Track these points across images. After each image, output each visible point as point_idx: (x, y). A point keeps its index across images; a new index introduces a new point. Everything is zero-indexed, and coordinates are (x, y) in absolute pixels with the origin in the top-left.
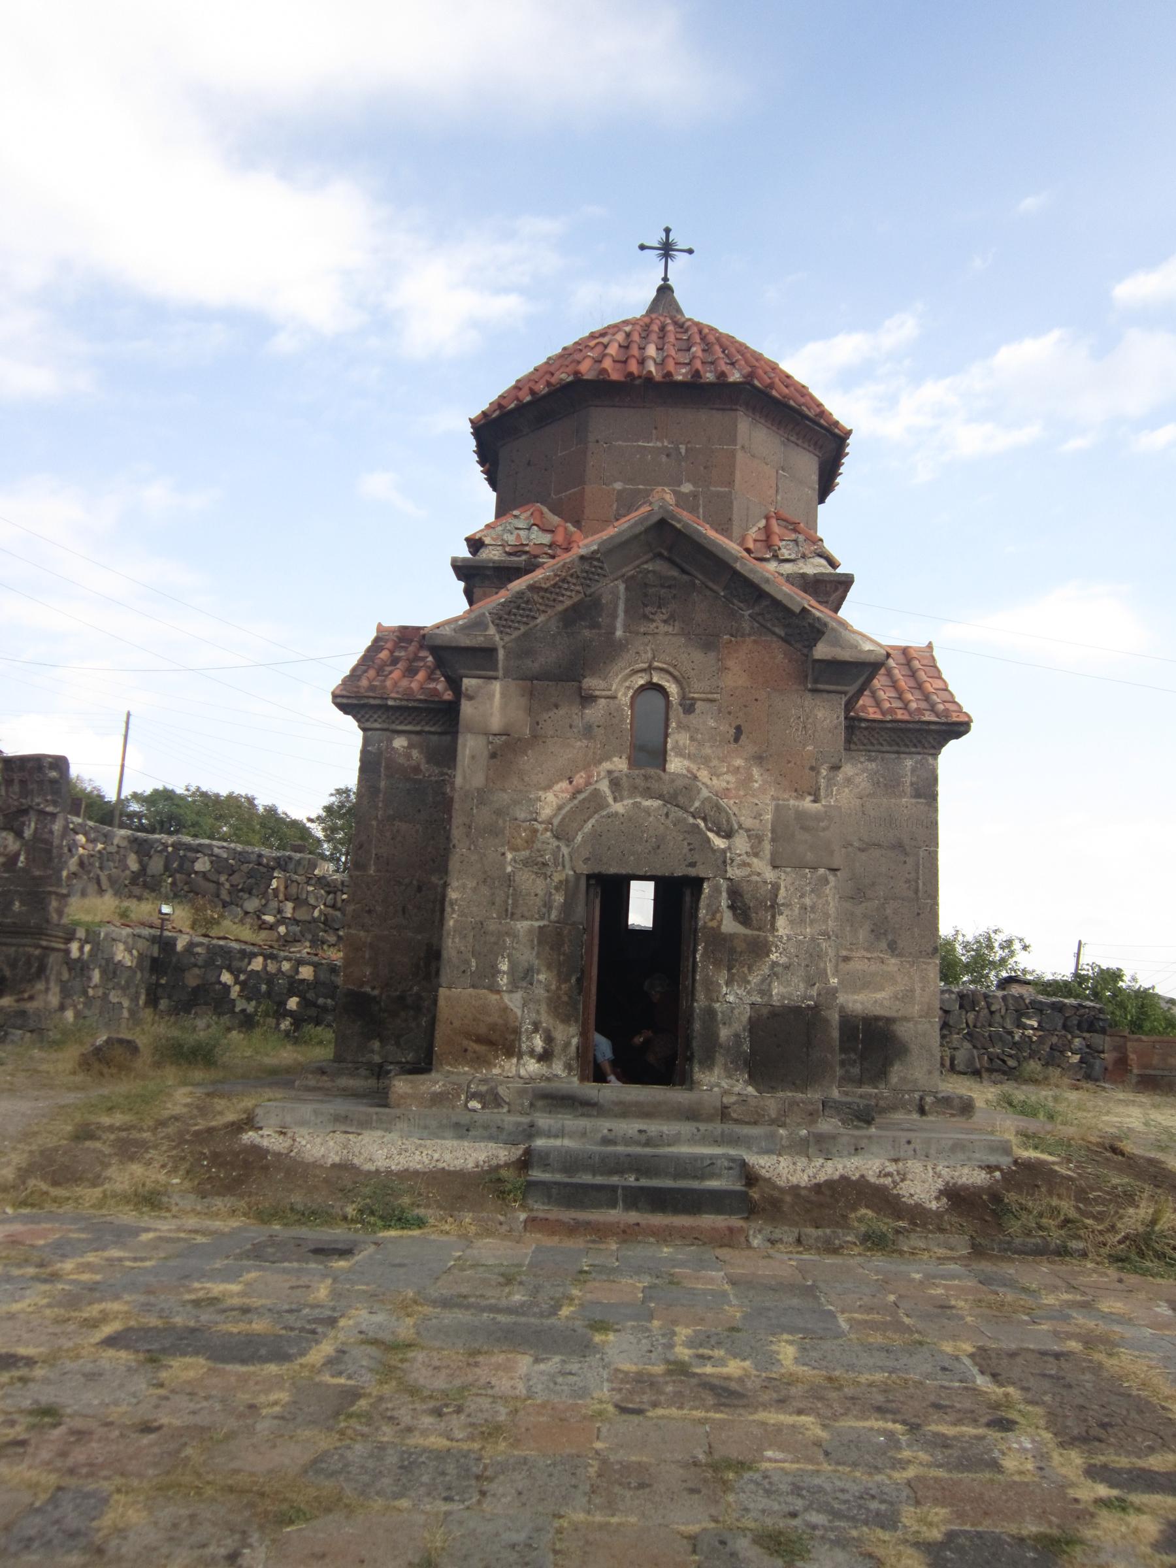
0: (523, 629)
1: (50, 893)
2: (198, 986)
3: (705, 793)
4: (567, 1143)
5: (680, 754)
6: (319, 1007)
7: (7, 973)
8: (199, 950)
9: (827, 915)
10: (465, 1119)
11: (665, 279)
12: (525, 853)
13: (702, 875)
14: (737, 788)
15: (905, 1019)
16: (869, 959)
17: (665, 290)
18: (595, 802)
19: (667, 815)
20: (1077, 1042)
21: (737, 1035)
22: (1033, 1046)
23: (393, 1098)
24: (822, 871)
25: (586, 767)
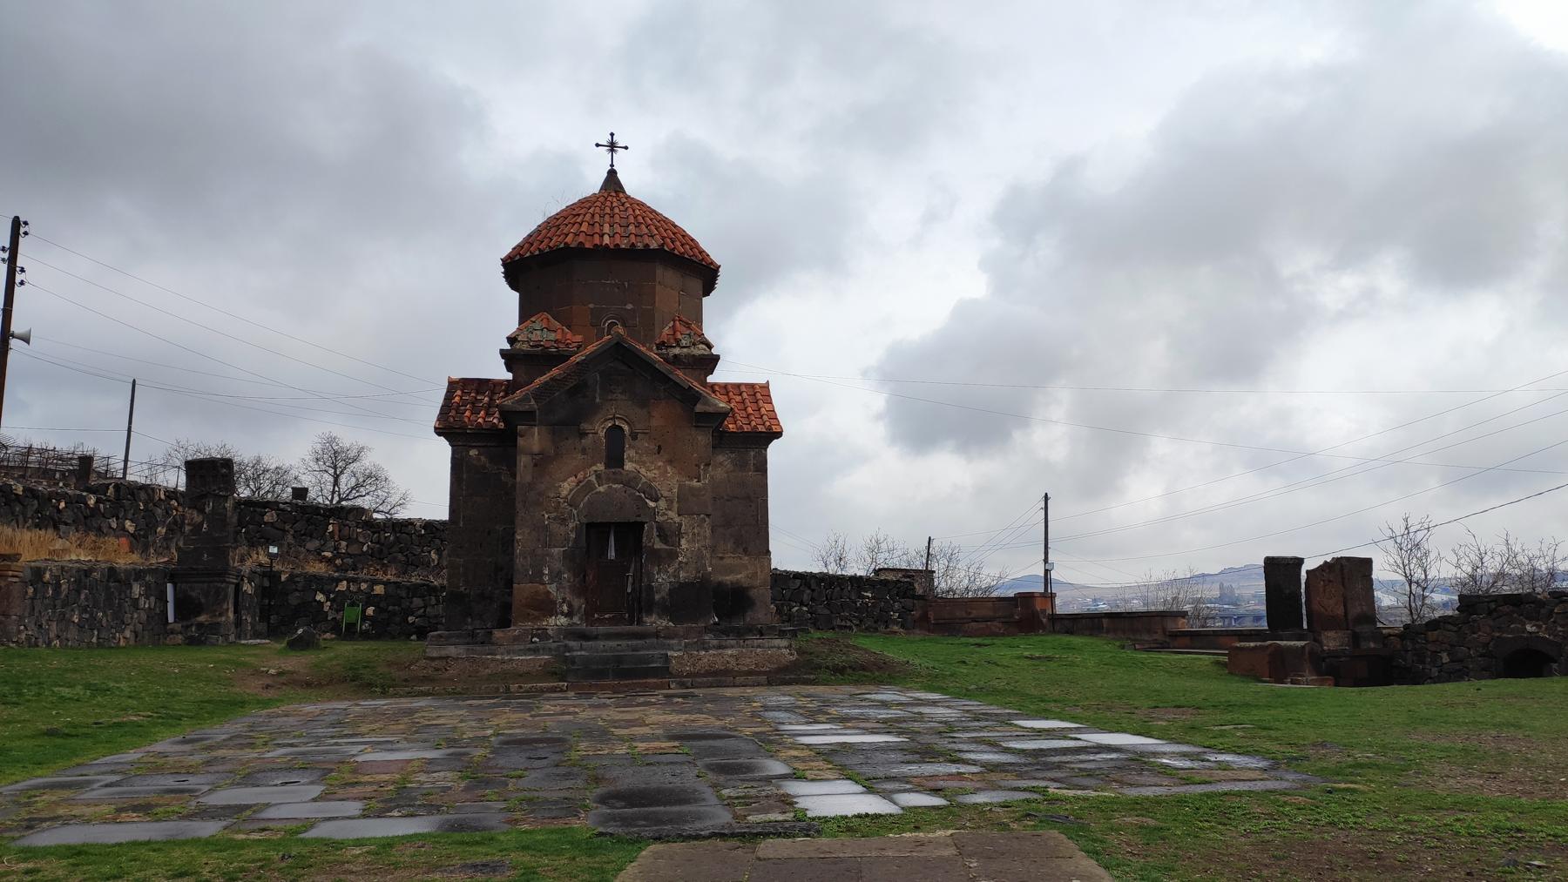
0: (548, 399)
2: (299, 604)
3: (644, 480)
4: (583, 653)
5: (631, 461)
7: (203, 601)
9: (705, 537)
10: (532, 646)
11: (612, 165)
13: (644, 521)
16: (734, 558)
17: (612, 173)
18: (589, 487)
20: (897, 605)
21: (663, 598)
23: (494, 640)
24: (702, 516)
25: (584, 469)
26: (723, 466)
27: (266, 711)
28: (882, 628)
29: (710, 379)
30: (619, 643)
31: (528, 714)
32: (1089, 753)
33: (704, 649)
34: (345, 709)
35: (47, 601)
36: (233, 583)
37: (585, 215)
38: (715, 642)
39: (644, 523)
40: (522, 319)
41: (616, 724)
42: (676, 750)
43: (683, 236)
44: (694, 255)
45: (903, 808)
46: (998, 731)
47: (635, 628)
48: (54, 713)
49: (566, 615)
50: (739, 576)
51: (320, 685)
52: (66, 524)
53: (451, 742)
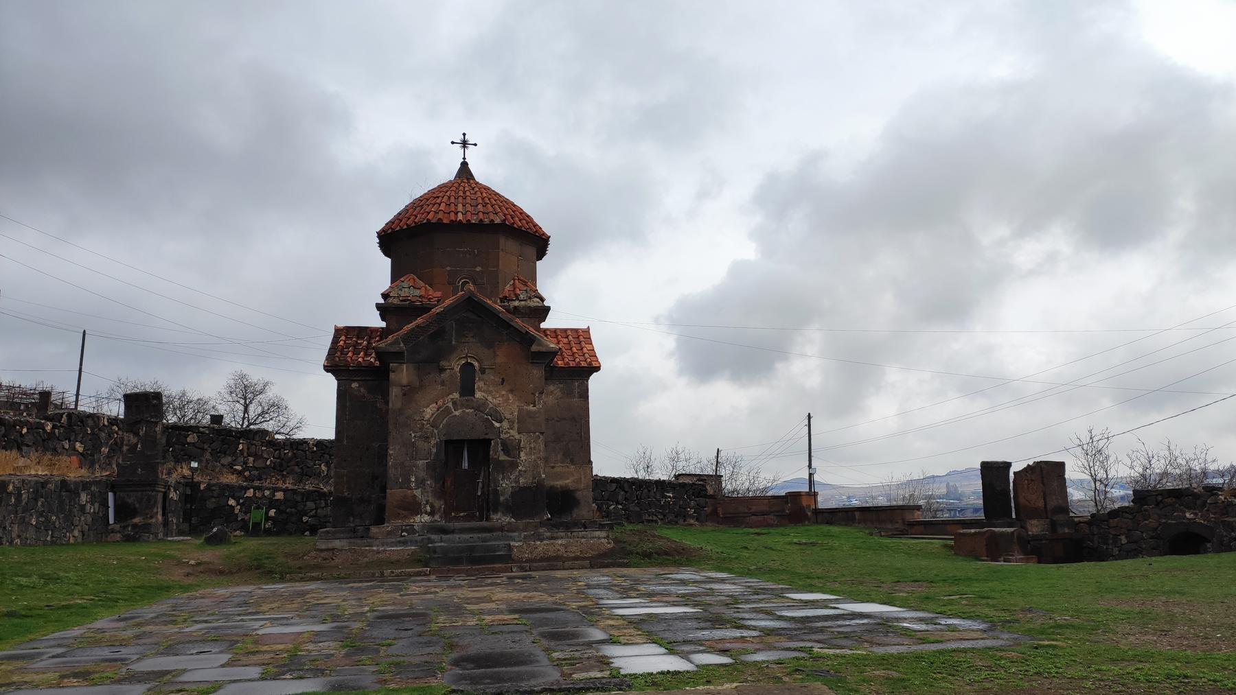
0: (414, 342)
1: (158, 463)
2: (215, 508)
3: (491, 406)
4: (443, 544)
6: (288, 513)
7: (137, 506)
8: (214, 488)
9: (540, 450)
10: (402, 539)
11: (464, 158)
12: (418, 434)
14: (503, 403)
15: (577, 490)
17: (464, 165)
19: (476, 415)
20: (693, 503)
21: (506, 499)
22: (671, 507)
23: (371, 534)
24: (537, 434)
25: (443, 398)
26: (553, 394)
27: (187, 594)
28: (681, 521)
29: (543, 325)
30: (471, 536)
31: (398, 594)
32: (846, 619)
33: (539, 540)
34: (250, 592)
35: (10, 508)
36: (161, 492)
37: (443, 197)
38: (548, 534)
39: (491, 440)
40: (393, 279)
41: (469, 601)
42: (516, 622)
43: (521, 213)
44: (530, 228)
45: (697, 666)
46: (773, 603)
47: (484, 523)
48: (13, 598)
49: (429, 514)
50: (567, 481)
51: (231, 573)
52: (28, 446)
53: (335, 618)
